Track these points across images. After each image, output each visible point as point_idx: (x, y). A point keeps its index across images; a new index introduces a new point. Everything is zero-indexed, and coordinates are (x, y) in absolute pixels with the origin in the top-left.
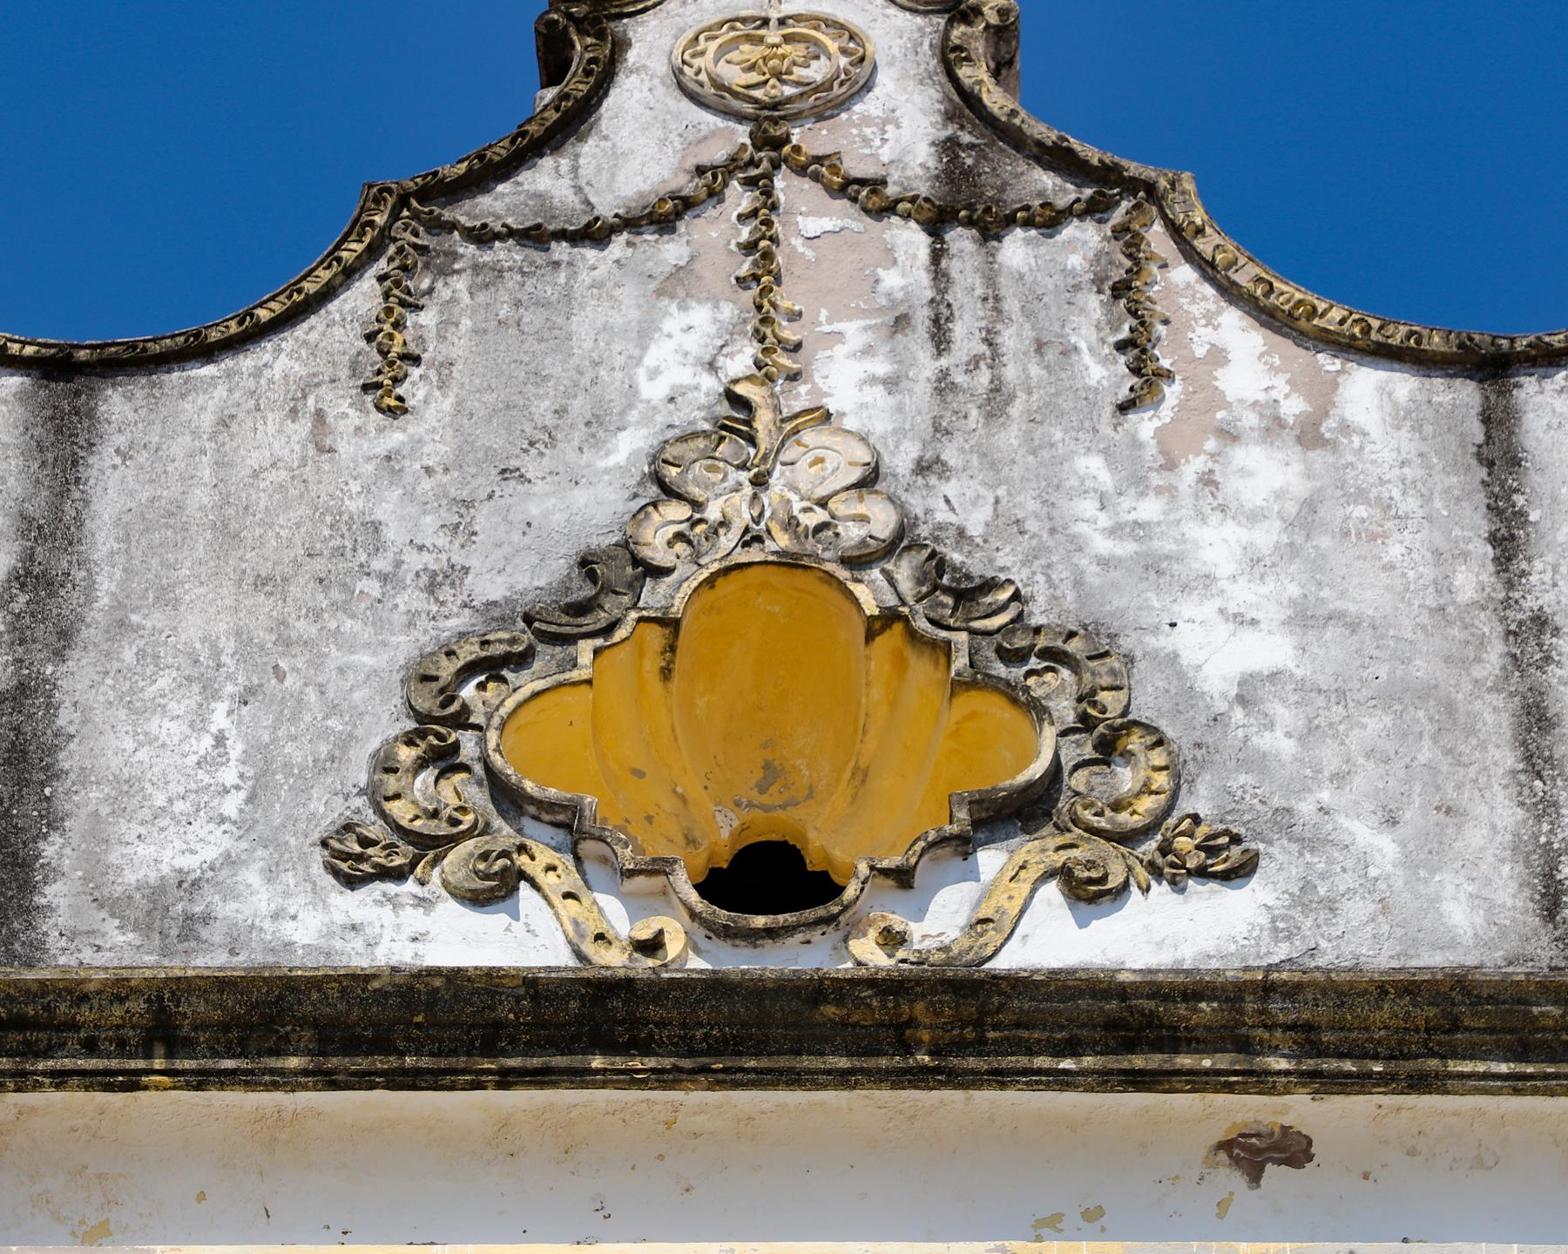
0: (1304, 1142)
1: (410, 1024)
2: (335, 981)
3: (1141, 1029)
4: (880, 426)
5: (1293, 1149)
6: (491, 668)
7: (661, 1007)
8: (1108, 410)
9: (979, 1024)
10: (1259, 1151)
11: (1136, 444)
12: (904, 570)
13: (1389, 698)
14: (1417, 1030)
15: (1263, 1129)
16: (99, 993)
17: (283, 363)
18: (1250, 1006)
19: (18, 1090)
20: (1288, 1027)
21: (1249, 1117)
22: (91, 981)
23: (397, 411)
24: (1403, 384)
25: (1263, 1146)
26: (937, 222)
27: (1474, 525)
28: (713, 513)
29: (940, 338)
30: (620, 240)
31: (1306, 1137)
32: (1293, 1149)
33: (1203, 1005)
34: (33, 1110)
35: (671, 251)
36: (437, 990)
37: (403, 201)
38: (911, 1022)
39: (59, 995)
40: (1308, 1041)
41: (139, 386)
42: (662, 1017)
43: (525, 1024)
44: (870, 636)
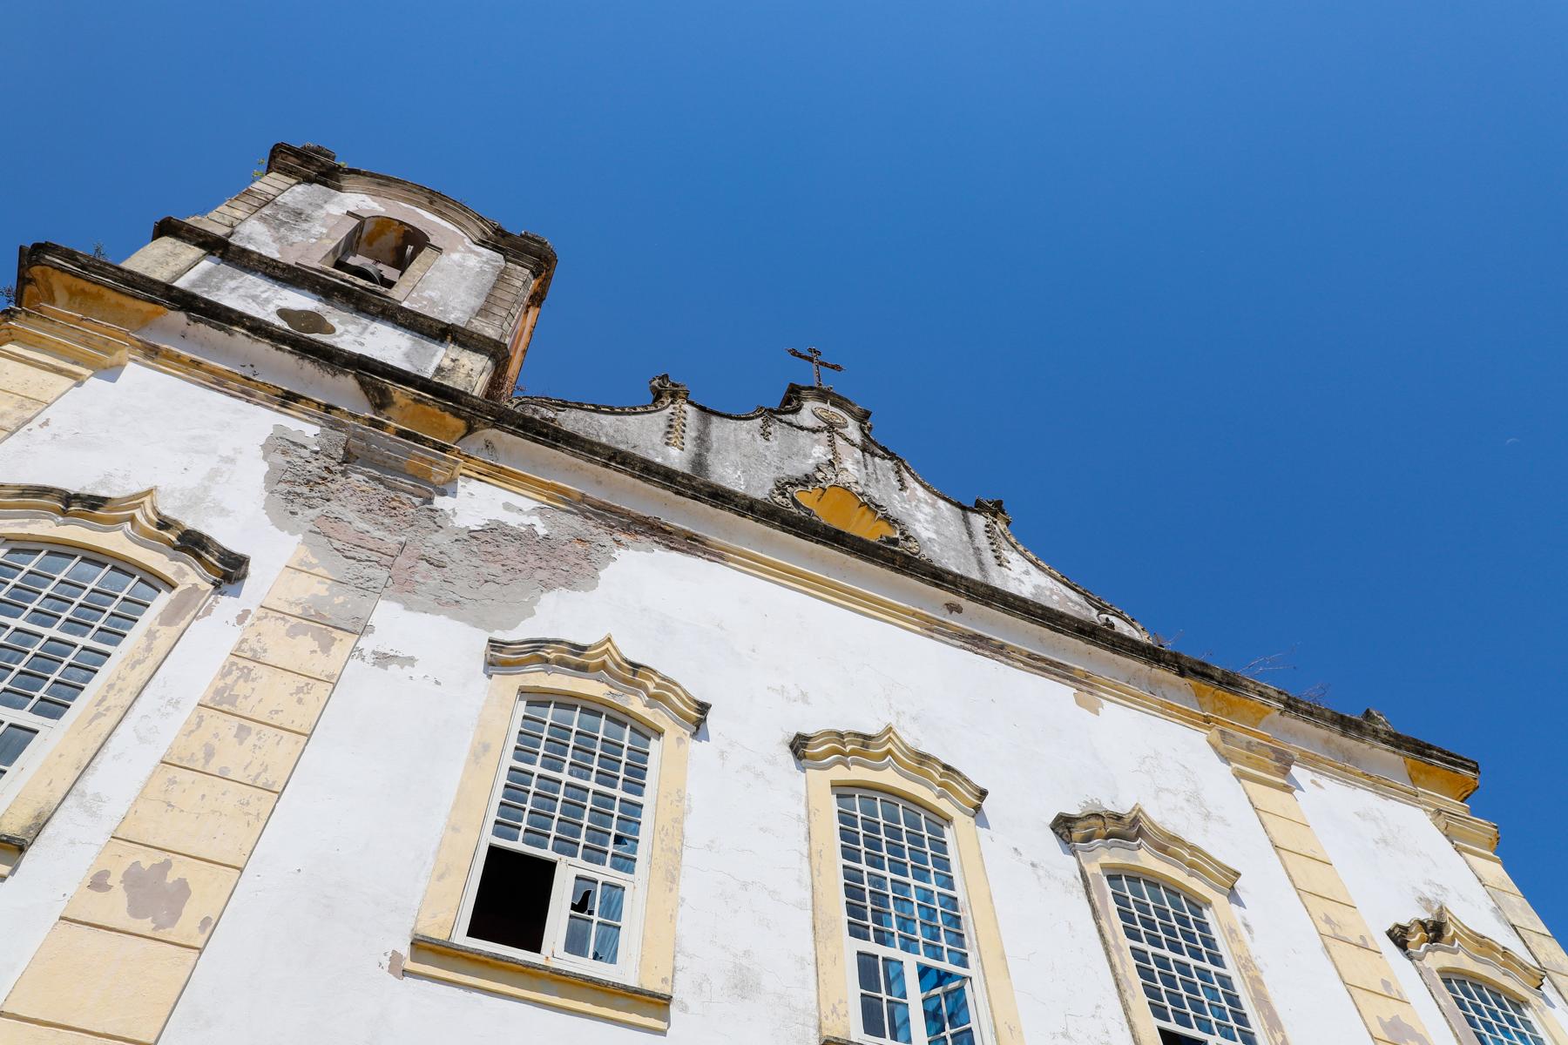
4: (857, 476)
6: (792, 485)
8: (897, 490)
11: (903, 496)
12: (866, 499)
13: (955, 550)
17: (745, 425)
23: (768, 440)
24: (948, 505)
26: (864, 450)
27: (965, 531)
28: (829, 477)
29: (866, 467)
30: (806, 432)
34: (721, 514)
35: (815, 436)
37: (766, 410)
41: (719, 418)
44: (860, 506)
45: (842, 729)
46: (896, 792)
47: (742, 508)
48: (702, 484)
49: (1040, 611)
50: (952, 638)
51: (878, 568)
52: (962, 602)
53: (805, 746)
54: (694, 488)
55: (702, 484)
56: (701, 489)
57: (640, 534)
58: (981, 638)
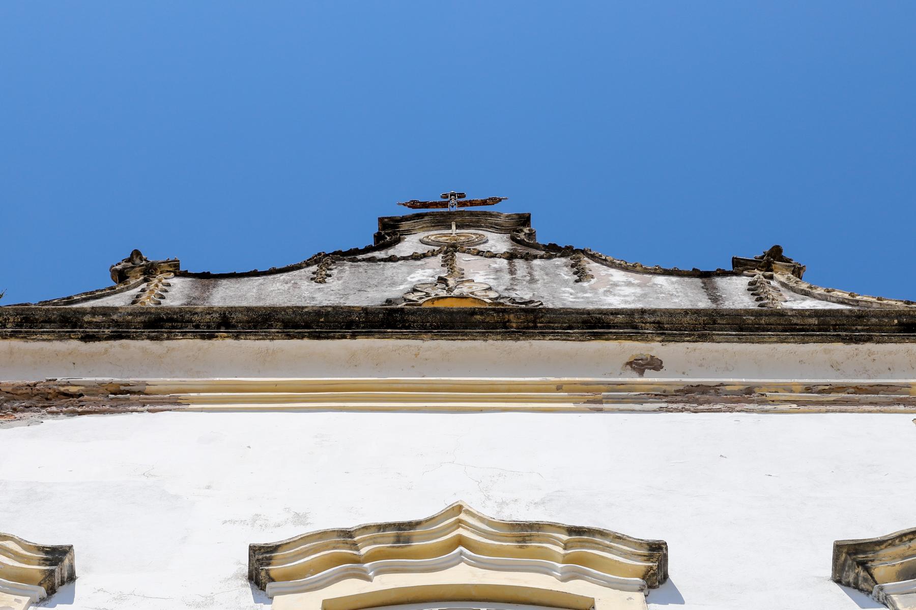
0: (660, 362)
1: (319, 322)
2: (291, 309)
3: (596, 323)
5: (655, 364)
7: (414, 316)
9: (534, 322)
10: (642, 365)
14: (700, 324)
15: (644, 357)
16: (202, 312)
18: (636, 316)
19: (168, 338)
20: (650, 323)
21: (638, 352)
22: (199, 308)
25: (644, 363)
30: (400, 262)
31: (660, 360)
32: (655, 364)
33: (619, 316)
34: (173, 349)
36: (329, 311)
38: (509, 321)
39: (187, 313)
40: (659, 327)
42: (414, 319)
43: (362, 322)
45: (350, 523)
46: (474, 593)
47: (209, 327)
48: (130, 314)
49: (814, 321)
50: (641, 403)
51: (479, 344)
52: (655, 348)
53: (268, 561)
54: (117, 324)
55: (130, 314)
56: (129, 322)
57: (23, 411)
58: (703, 389)
